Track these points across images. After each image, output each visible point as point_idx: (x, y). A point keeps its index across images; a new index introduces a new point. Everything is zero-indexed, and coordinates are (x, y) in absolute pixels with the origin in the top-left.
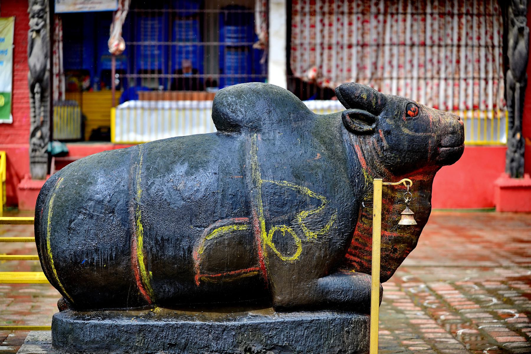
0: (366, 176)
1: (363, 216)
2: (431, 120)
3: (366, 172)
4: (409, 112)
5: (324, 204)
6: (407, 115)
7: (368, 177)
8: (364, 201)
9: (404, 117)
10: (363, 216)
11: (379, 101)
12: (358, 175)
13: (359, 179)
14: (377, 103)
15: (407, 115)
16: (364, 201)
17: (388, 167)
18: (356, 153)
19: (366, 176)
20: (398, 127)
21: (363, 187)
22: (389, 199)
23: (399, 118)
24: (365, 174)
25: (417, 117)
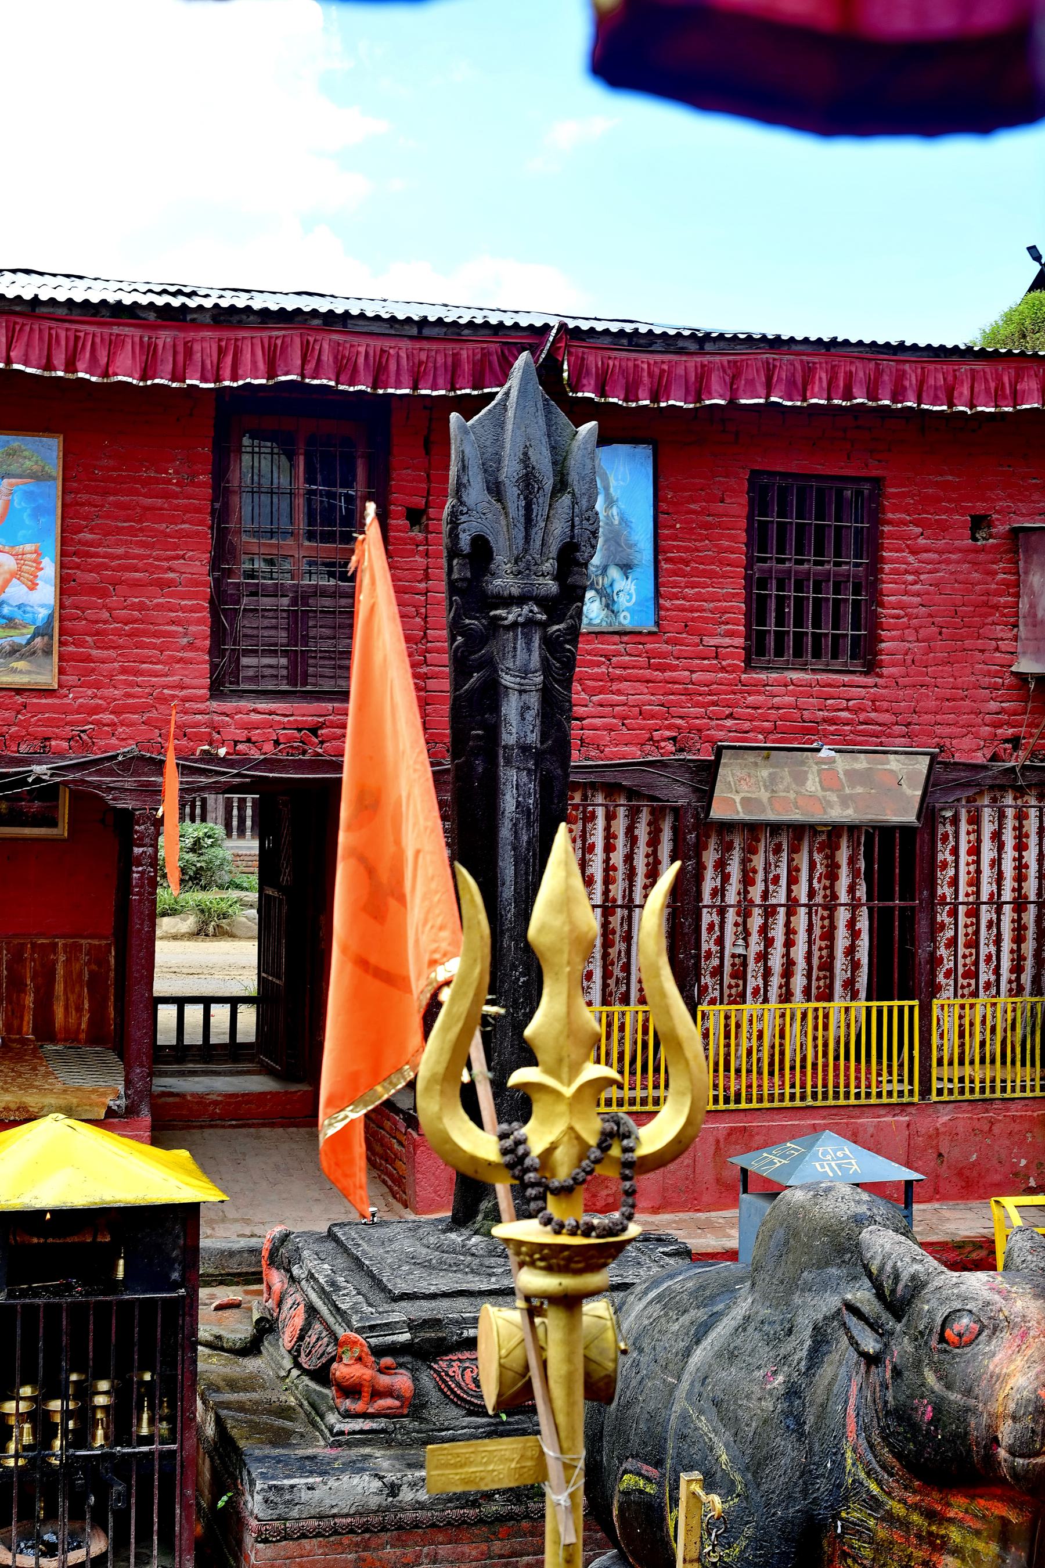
0: (849, 1461)
1: (845, 1555)
2: (991, 1367)
3: (854, 1450)
4: (948, 1332)
5: (738, 1495)
6: (942, 1339)
7: (853, 1464)
8: (842, 1519)
9: (934, 1343)
10: (849, 1555)
11: (900, 1286)
12: (835, 1454)
13: (833, 1462)
14: (893, 1291)
15: (942, 1339)
16: (842, 1519)
17: (898, 1456)
18: (846, 1402)
19: (849, 1461)
20: (918, 1365)
21: (839, 1486)
22: (918, 1536)
23: (926, 1343)
24: (849, 1454)
25: (967, 1350)
